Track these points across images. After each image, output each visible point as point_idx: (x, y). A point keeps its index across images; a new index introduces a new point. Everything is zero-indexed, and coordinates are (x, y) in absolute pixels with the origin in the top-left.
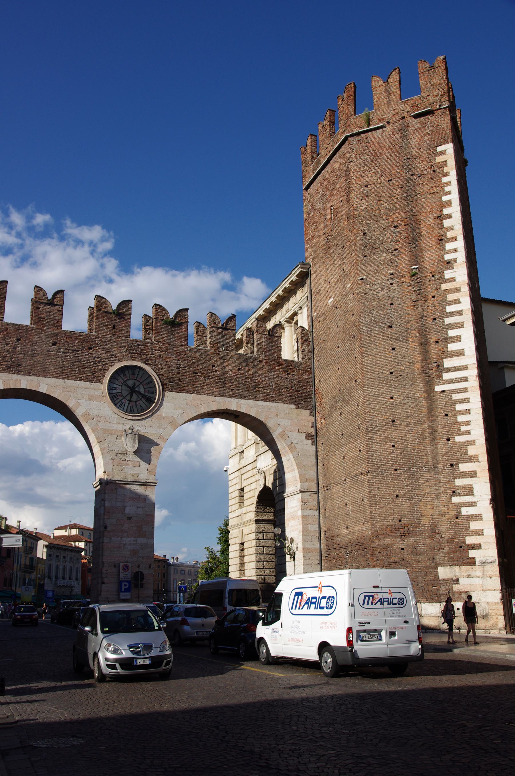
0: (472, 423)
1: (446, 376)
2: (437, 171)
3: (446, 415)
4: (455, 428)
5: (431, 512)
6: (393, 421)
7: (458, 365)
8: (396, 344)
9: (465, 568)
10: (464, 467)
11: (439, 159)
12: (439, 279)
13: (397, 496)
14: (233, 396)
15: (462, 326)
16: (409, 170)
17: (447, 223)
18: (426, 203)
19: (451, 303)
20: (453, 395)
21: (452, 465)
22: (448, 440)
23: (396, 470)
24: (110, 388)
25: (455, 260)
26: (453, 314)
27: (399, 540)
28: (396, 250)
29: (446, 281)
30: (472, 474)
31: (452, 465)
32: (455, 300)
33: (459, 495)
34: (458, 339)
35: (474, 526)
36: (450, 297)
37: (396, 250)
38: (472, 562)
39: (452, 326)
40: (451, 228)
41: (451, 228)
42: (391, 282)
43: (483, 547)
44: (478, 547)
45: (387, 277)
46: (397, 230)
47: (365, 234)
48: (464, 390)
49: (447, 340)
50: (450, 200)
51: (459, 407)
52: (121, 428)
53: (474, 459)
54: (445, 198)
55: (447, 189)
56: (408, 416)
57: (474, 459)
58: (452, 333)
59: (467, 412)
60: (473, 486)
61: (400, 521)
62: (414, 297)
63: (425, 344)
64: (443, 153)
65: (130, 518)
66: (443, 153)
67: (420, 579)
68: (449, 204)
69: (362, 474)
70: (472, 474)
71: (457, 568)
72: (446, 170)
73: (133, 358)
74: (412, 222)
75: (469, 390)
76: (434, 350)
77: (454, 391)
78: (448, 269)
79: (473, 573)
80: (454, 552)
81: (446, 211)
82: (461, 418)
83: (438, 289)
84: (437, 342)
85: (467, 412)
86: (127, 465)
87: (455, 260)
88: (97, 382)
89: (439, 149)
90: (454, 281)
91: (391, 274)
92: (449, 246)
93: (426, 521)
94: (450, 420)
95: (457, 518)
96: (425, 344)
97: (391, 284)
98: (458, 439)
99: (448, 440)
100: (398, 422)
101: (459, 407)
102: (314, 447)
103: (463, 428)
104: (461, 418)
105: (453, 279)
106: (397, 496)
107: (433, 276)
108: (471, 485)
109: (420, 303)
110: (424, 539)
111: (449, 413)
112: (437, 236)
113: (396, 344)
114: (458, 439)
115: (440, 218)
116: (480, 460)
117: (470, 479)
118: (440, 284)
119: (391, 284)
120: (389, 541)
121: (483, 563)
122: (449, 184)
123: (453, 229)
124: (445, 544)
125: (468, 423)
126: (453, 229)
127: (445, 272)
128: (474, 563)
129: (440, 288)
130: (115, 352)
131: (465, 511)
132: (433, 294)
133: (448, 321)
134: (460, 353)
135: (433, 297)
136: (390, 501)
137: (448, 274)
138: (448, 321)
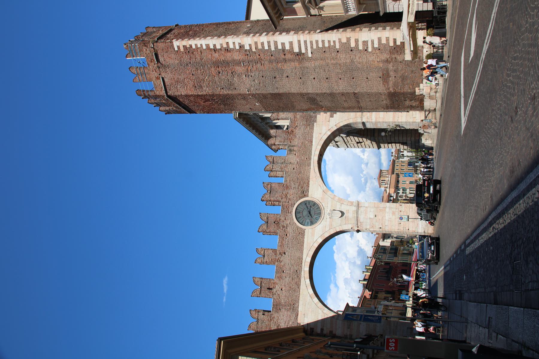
1: (303, 51)
2: (188, 50)
5: (376, 62)
8: (285, 75)
10: (353, 45)
11: (182, 49)
14: (310, 159)
15: (276, 42)
16: (187, 64)
17: (218, 47)
18: (207, 56)
19: (263, 47)
22: (338, 52)
24: (308, 225)
25: (239, 44)
26: (269, 46)
27: (390, 79)
30: (357, 41)
34: (283, 44)
35: (384, 41)
36: (260, 47)
38: (403, 43)
39: (276, 47)
40: (221, 45)
41: (221, 45)
44: (395, 41)
45: (247, 78)
48: (311, 43)
49: (283, 50)
51: (320, 45)
53: (349, 39)
54: (204, 47)
55: (199, 46)
56: (325, 71)
57: (349, 39)
58: (280, 47)
59: (323, 41)
62: (259, 65)
64: (178, 47)
66: (178, 47)
67: (411, 69)
70: (357, 41)
72: (188, 46)
73: (291, 212)
74: (217, 64)
76: (288, 56)
77: (312, 47)
80: (398, 52)
81: (212, 47)
82: (327, 45)
85: (323, 41)
87: (239, 44)
88: (304, 232)
89: (176, 49)
92: (231, 46)
93: (381, 65)
94: (327, 50)
98: (337, 47)
99: (338, 52)
100: (328, 76)
101: (320, 45)
103: (332, 44)
104: (327, 45)
105: (250, 45)
109: (263, 62)
110: (390, 66)
112: (225, 52)
114: (337, 47)
115: (215, 50)
120: (391, 84)
122: (196, 45)
124: (393, 56)
125: (329, 42)
128: (404, 43)
131: (376, 45)
133: (273, 49)
134: (291, 43)
136: (370, 82)
137: (247, 47)
138: (273, 49)
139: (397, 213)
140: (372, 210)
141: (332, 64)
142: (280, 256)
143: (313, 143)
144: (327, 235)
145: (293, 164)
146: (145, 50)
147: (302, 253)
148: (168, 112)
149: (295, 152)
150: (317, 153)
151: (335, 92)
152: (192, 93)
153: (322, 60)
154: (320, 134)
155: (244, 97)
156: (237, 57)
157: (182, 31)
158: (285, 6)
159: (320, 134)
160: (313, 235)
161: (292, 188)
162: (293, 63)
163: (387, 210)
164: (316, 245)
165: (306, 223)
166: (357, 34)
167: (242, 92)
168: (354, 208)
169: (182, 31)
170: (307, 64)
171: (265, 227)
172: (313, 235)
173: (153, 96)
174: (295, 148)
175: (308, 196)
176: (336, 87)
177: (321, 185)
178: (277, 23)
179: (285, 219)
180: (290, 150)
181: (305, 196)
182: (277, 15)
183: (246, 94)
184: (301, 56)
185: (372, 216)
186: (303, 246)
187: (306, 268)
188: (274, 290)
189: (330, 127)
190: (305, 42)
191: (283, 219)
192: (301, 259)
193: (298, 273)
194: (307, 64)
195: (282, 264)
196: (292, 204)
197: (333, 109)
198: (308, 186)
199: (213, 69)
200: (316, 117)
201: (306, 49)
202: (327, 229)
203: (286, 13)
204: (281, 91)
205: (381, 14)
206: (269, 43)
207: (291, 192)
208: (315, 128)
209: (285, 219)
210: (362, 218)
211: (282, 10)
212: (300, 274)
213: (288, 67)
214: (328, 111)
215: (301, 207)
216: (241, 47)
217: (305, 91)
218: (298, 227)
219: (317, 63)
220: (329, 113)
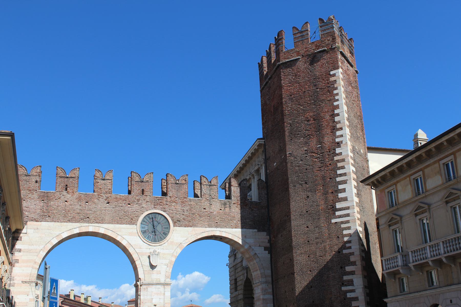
0: (352, 241)
1: (337, 213)
2: (330, 88)
3: (338, 237)
7: (345, 206)
8: (309, 194)
10: (348, 269)
11: (332, 79)
13: (311, 287)
14: (216, 227)
17: (337, 119)
20: (342, 225)
21: (341, 268)
25: (342, 142)
26: (341, 175)
29: (338, 155)
30: (352, 273)
31: (341, 268)
33: (346, 286)
34: (344, 190)
36: (339, 165)
40: (339, 122)
48: (348, 222)
53: (354, 263)
54: (335, 104)
56: (317, 238)
58: (340, 187)
61: (313, 302)
65: (155, 305)
68: (337, 107)
70: (352, 273)
72: (335, 86)
74: (317, 119)
75: (350, 221)
76: (331, 197)
77: (342, 223)
81: (336, 112)
83: (333, 160)
86: (153, 273)
87: (342, 142)
88: (133, 224)
89: (332, 73)
92: (338, 133)
100: (311, 242)
106: (311, 287)
108: (352, 279)
109: (322, 169)
113: (309, 194)
115: (333, 115)
116: (357, 264)
117: (351, 276)
118: (333, 156)
122: (337, 94)
123: (340, 123)
126: (340, 123)
127: (336, 149)
129: (334, 159)
131: (349, 295)
133: (338, 179)
134: (345, 199)
137: (338, 151)
138: (338, 179)
140: (162, 301)
141: (325, 246)
143: (234, 230)
144: (131, 250)
145: (210, 208)
146: (329, 39)
147: (109, 223)
148: (261, 66)
150: (224, 235)
151: (294, 251)
152: (283, 92)
153: (329, 234)
155: (283, 149)
156: (327, 140)
157: (352, 78)
158: (387, 191)
160: (131, 234)
161: (183, 208)
162: (323, 203)
164: (118, 238)
166: (361, 273)
167: (288, 147)
169: (352, 78)
170: (322, 219)
171: (137, 179)
172: (130, 235)
173: (279, 50)
174: (227, 210)
176: (299, 252)
177: (187, 241)
178: (367, 182)
179: (147, 202)
180: (225, 204)
181: (175, 223)
182: (376, 182)
183: (286, 152)
184: (333, 210)
185: (154, 302)
186: (118, 223)
187: (91, 228)
188: (65, 193)
189: (253, 247)
190: (348, 215)
191: (148, 199)
192: (102, 221)
193: (86, 219)
194: (322, 219)
196: (164, 208)
199: (311, 114)
200: (263, 231)
201: (340, 217)
203: (379, 193)
204: (291, 191)
205: (385, 300)
206: (345, 174)
207: (179, 207)
208: (251, 230)
209: (147, 202)
210: (152, 289)
211: (382, 187)
212: (85, 222)
213: (318, 197)
214: (271, 244)
215: (162, 220)
216: (339, 144)
217: (292, 217)
218: (138, 216)
219: (325, 231)
220: (268, 245)
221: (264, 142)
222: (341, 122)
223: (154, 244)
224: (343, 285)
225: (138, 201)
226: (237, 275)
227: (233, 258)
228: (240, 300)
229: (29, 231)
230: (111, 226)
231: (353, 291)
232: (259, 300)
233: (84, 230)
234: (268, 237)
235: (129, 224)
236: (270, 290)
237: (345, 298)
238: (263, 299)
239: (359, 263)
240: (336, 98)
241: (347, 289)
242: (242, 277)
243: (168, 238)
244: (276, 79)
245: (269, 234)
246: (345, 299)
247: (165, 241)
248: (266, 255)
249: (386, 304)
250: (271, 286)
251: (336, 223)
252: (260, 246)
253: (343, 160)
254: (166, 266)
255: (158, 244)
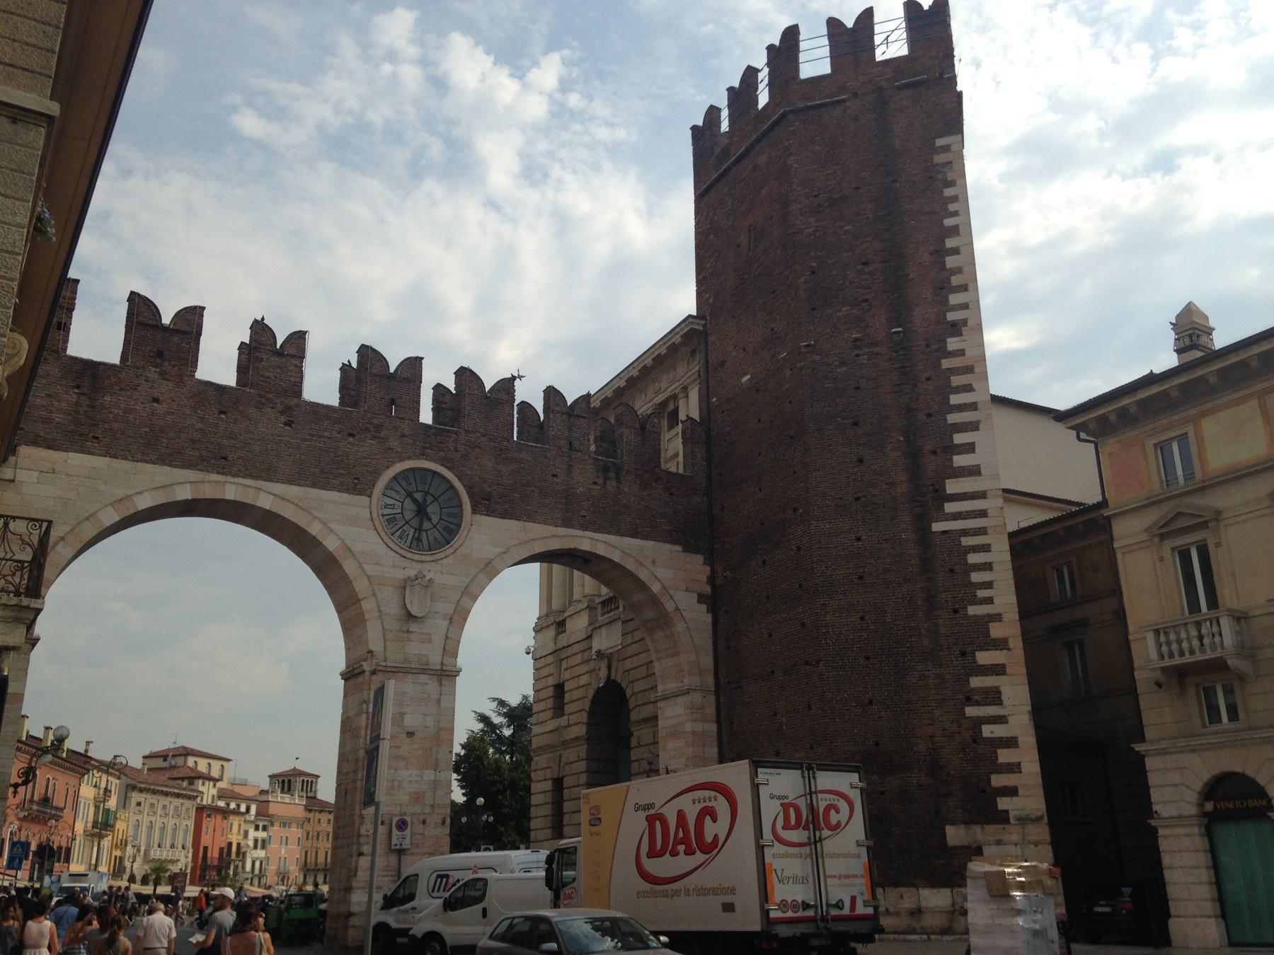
0: (995, 584)
1: (950, 507)
3: (952, 571)
4: (969, 593)
6: (861, 578)
9: (990, 828)
10: (984, 658)
12: (937, 351)
13: (871, 703)
17: (951, 262)
23: (867, 658)
25: (965, 322)
26: (960, 408)
28: (866, 301)
30: (998, 670)
31: (963, 654)
32: (964, 386)
33: (978, 704)
34: (970, 448)
35: (1004, 756)
36: (956, 381)
37: (866, 301)
38: (1003, 818)
42: (856, 352)
43: (1020, 792)
44: (1012, 792)
46: (867, 269)
47: (813, 272)
48: (982, 531)
50: (957, 226)
51: (973, 558)
52: (401, 574)
53: (1002, 644)
54: (948, 222)
57: (1002, 644)
58: (959, 438)
59: (988, 567)
60: (1002, 689)
61: (877, 744)
63: (913, 455)
65: (410, 734)
69: (806, 664)
70: (998, 670)
71: (977, 829)
73: (423, 455)
75: (989, 531)
77: (965, 533)
78: (953, 335)
79: (1006, 837)
81: (950, 243)
82: (976, 577)
84: (934, 452)
85: (988, 567)
86: (409, 640)
87: (965, 322)
88: (361, 493)
89: (940, 142)
90: (964, 355)
91: (856, 340)
92: (954, 299)
95: (975, 741)
96: (913, 455)
97: (858, 356)
98: (973, 610)
99: (956, 611)
101: (973, 558)
102: (709, 618)
103: (981, 594)
104: (976, 577)
105: (961, 353)
106: (871, 703)
107: (927, 346)
111: (956, 568)
114: (973, 610)
115: (941, 253)
117: (994, 678)
119: (858, 356)
121: (1022, 820)
125: (988, 585)
128: (1007, 821)
129: (940, 365)
130: (394, 443)
131: (987, 731)
132: (927, 375)
133: (952, 418)
134: (975, 471)
135: (928, 379)
137: (953, 344)
138: (952, 418)
139: (418, 809)
140: (430, 722)
142: (280, 407)
143: (628, 541)
147: (290, 482)
149: (601, 481)
154: (654, 562)
159: (654, 562)
163: (429, 775)
164: (315, 529)
165: (390, 501)
168: (435, 660)
174: (612, 484)
175: (474, 511)
179: (403, 436)
186: (314, 485)
187: (232, 489)
188: (152, 372)
189: (672, 592)
190: (983, 514)
192: (269, 473)
193: (218, 461)
195: (252, 411)
197: (715, 600)
198: (504, 515)
200: (697, 551)
202: (369, 569)
208: (668, 546)
209: (403, 436)
218: (377, 473)
220: (707, 589)
221: (704, 326)
222: (965, 269)
223: (417, 557)
224: (969, 700)
225: (378, 431)
226: (567, 675)
227: (551, 632)
228: (577, 738)
229: (22, 475)
230: (294, 491)
231: (1001, 720)
232: (676, 733)
233: (208, 492)
234: (708, 569)
235: (348, 491)
236: (711, 710)
237: (977, 738)
238: (694, 733)
239: (1017, 644)
240: (952, 207)
241: (981, 714)
242: (584, 680)
243: (456, 542)
244: (762, 159)
245: (710, 561)
246: (975, 741)
247: (448, 552)
248: (699, 616)
249: (1140, 759)
250: (712, 699)
251: (945, 532)
252: (687, 590)
253: (969, 370)
254: (446, 623)
255: (428, 558)
